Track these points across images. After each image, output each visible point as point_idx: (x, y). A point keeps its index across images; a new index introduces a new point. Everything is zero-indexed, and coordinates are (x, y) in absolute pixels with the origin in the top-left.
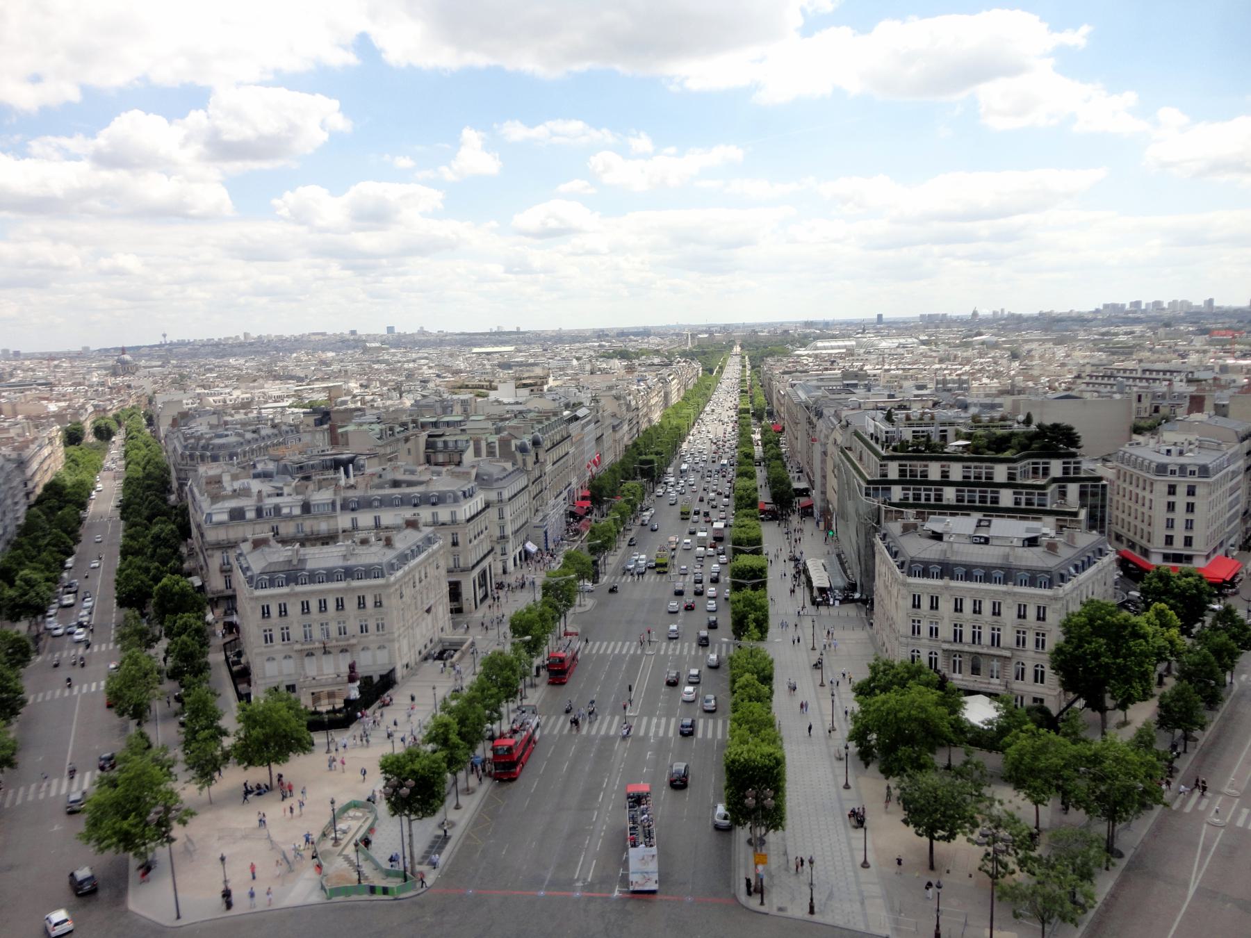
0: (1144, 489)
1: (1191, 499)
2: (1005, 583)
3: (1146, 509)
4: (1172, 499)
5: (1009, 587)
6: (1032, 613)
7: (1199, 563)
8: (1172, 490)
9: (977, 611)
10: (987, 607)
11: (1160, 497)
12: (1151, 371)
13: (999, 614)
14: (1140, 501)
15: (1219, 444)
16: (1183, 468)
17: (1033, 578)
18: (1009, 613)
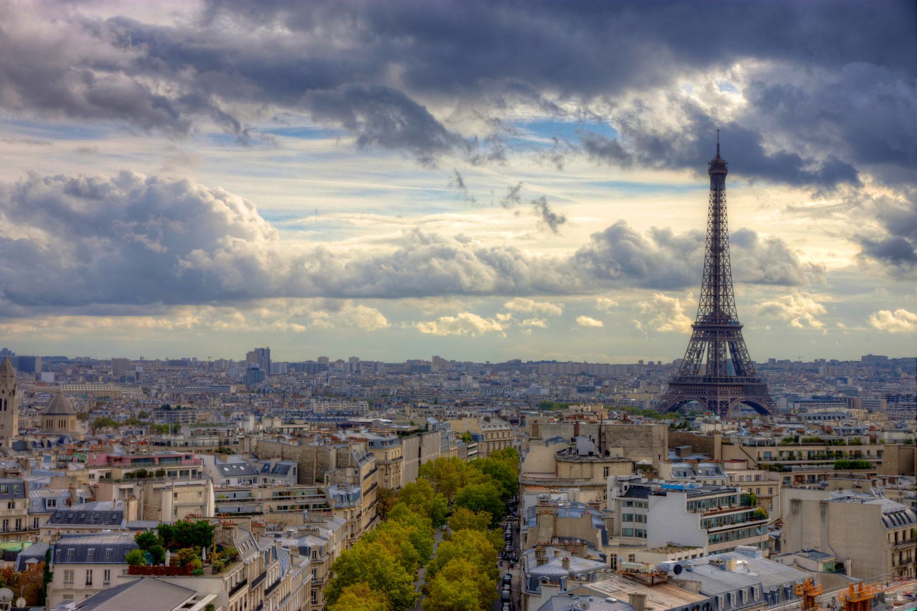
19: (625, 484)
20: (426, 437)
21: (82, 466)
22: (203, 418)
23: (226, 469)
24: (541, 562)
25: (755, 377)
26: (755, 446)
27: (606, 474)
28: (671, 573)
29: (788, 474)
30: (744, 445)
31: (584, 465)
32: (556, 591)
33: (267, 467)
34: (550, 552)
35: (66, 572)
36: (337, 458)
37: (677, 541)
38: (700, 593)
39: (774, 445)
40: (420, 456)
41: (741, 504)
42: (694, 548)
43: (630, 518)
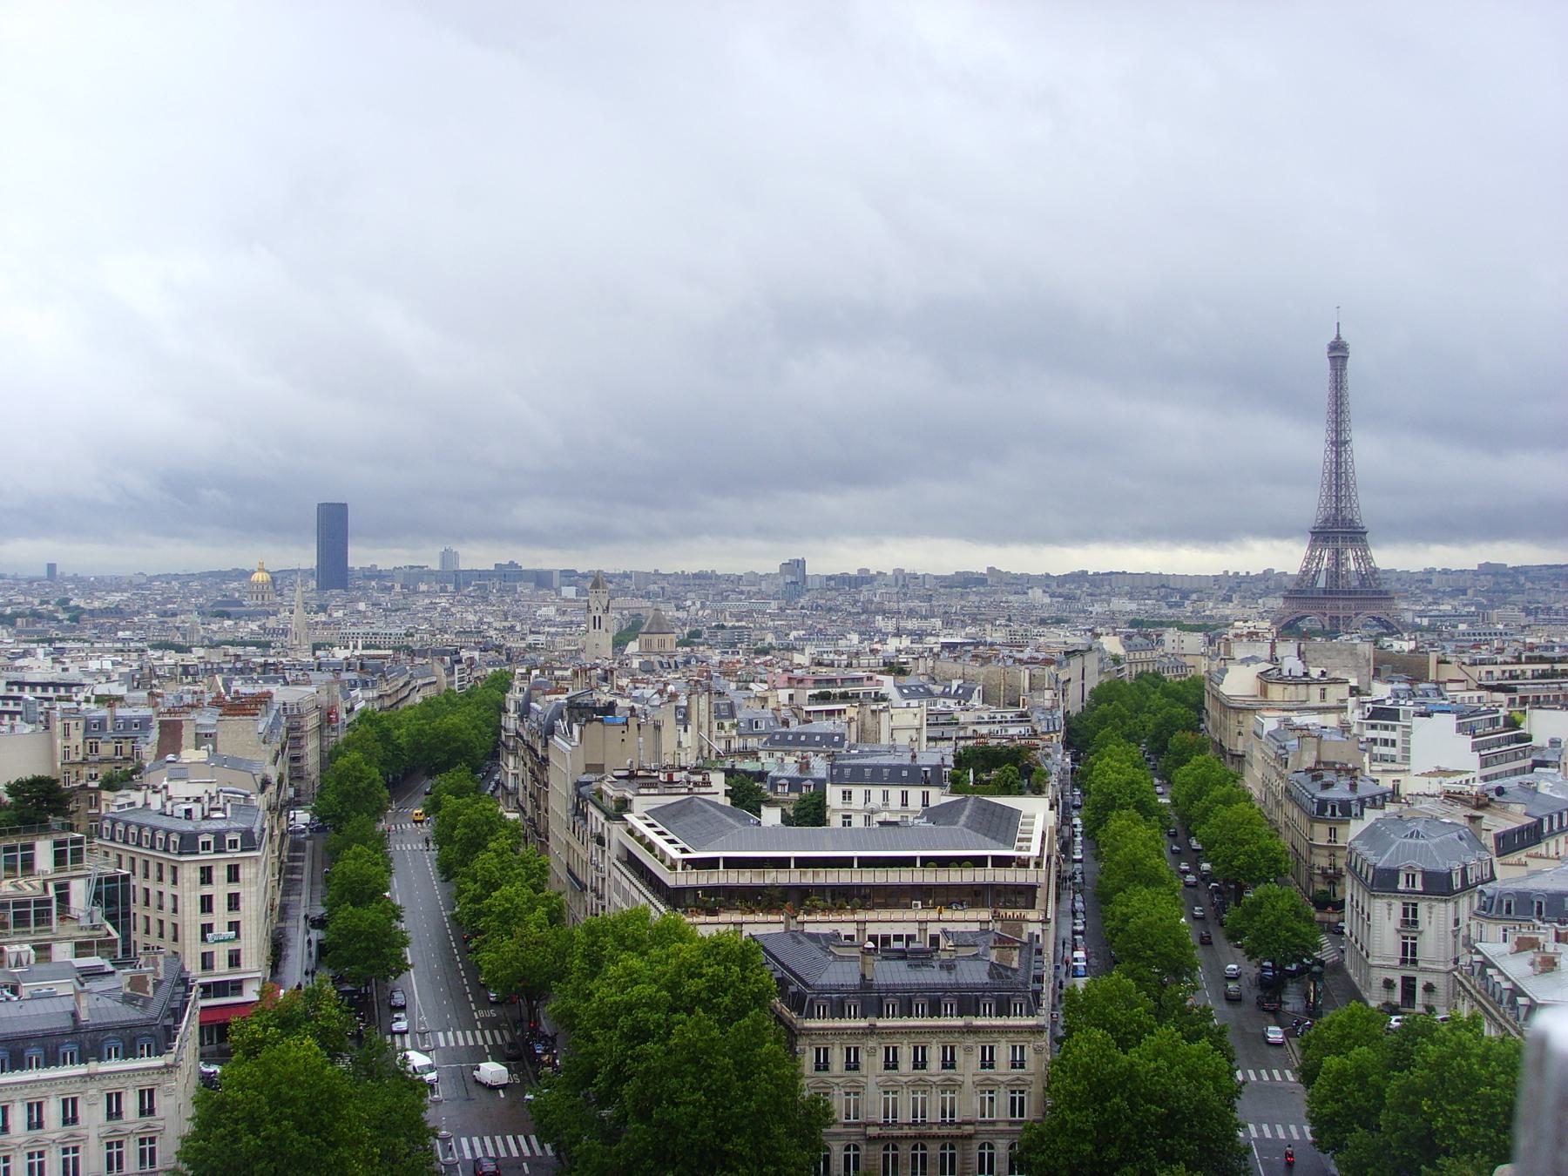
0: (160, 879)
1: (234, 888)
2: (83, 1060)
3: (166, 915)
4: (207, 890)
5: (94, 1066)
6: (130, 1104)
7: (250, 994)
8: (206, 876)
9: (36, 1123)
10: (53, 1111)
11: (189, 889)
12: (21, 685)
13: (75, 1120)
14: (153, 901)
15: (247, 796)
16: (219, 836)
17: (130, 1040)
18: (93, 1116)
19: (1369, 705)
20: (1088, 657)
21: (765, 686)
22: (760, 637)
23: (905, 691)
24: (1327, 786)
25: (1381, 588)
26: (1476, 665)
27: (1323, 696)
28: (1492, 795)
29: (1512, 695)
30: (1464, 663)
31: (1300, 686)
32: (1378, 814)
33: (947, 690)
34: (1329, 777)
35: (844, 792)
36: (1030, 679)
37: (1444, 766)
38: (1526, 814)
39: (1496, 663)
40: (1083, 679)
41: (1505, 726)
42: (1468, 772)
43: (1374, 741)
